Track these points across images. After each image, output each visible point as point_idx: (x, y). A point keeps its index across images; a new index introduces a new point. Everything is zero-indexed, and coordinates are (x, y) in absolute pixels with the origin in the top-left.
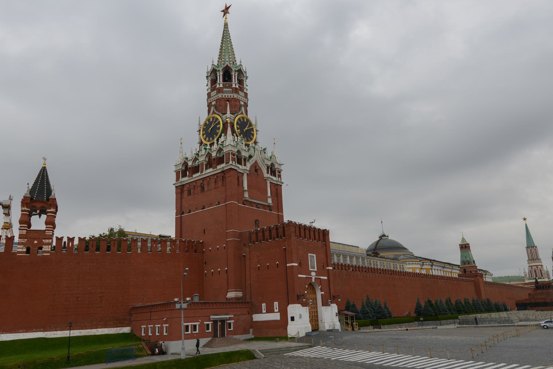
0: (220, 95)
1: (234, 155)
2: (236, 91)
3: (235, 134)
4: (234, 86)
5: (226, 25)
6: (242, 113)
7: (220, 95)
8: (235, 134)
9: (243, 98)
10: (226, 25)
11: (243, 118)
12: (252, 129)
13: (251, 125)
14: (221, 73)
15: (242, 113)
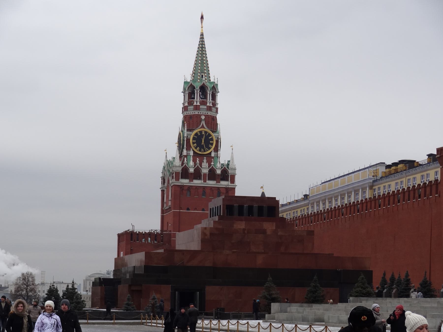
0: (185, 113)
1: (177, 174)
2: (197, 108)
3: (191, 150)
4: (195, 104)
5: (202, 35)
6: (203, 127)
7: (185, 113)
8: (191, 150)
9: (204, 112)
10: (202, 35)
11: (201, 132)
12: (212, 139)
13: (210, 135)
14: (187, 92)
15: (203, 127)
